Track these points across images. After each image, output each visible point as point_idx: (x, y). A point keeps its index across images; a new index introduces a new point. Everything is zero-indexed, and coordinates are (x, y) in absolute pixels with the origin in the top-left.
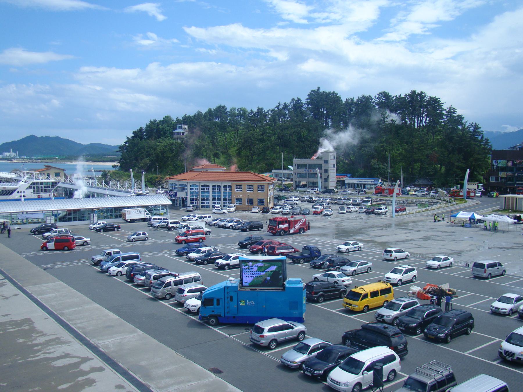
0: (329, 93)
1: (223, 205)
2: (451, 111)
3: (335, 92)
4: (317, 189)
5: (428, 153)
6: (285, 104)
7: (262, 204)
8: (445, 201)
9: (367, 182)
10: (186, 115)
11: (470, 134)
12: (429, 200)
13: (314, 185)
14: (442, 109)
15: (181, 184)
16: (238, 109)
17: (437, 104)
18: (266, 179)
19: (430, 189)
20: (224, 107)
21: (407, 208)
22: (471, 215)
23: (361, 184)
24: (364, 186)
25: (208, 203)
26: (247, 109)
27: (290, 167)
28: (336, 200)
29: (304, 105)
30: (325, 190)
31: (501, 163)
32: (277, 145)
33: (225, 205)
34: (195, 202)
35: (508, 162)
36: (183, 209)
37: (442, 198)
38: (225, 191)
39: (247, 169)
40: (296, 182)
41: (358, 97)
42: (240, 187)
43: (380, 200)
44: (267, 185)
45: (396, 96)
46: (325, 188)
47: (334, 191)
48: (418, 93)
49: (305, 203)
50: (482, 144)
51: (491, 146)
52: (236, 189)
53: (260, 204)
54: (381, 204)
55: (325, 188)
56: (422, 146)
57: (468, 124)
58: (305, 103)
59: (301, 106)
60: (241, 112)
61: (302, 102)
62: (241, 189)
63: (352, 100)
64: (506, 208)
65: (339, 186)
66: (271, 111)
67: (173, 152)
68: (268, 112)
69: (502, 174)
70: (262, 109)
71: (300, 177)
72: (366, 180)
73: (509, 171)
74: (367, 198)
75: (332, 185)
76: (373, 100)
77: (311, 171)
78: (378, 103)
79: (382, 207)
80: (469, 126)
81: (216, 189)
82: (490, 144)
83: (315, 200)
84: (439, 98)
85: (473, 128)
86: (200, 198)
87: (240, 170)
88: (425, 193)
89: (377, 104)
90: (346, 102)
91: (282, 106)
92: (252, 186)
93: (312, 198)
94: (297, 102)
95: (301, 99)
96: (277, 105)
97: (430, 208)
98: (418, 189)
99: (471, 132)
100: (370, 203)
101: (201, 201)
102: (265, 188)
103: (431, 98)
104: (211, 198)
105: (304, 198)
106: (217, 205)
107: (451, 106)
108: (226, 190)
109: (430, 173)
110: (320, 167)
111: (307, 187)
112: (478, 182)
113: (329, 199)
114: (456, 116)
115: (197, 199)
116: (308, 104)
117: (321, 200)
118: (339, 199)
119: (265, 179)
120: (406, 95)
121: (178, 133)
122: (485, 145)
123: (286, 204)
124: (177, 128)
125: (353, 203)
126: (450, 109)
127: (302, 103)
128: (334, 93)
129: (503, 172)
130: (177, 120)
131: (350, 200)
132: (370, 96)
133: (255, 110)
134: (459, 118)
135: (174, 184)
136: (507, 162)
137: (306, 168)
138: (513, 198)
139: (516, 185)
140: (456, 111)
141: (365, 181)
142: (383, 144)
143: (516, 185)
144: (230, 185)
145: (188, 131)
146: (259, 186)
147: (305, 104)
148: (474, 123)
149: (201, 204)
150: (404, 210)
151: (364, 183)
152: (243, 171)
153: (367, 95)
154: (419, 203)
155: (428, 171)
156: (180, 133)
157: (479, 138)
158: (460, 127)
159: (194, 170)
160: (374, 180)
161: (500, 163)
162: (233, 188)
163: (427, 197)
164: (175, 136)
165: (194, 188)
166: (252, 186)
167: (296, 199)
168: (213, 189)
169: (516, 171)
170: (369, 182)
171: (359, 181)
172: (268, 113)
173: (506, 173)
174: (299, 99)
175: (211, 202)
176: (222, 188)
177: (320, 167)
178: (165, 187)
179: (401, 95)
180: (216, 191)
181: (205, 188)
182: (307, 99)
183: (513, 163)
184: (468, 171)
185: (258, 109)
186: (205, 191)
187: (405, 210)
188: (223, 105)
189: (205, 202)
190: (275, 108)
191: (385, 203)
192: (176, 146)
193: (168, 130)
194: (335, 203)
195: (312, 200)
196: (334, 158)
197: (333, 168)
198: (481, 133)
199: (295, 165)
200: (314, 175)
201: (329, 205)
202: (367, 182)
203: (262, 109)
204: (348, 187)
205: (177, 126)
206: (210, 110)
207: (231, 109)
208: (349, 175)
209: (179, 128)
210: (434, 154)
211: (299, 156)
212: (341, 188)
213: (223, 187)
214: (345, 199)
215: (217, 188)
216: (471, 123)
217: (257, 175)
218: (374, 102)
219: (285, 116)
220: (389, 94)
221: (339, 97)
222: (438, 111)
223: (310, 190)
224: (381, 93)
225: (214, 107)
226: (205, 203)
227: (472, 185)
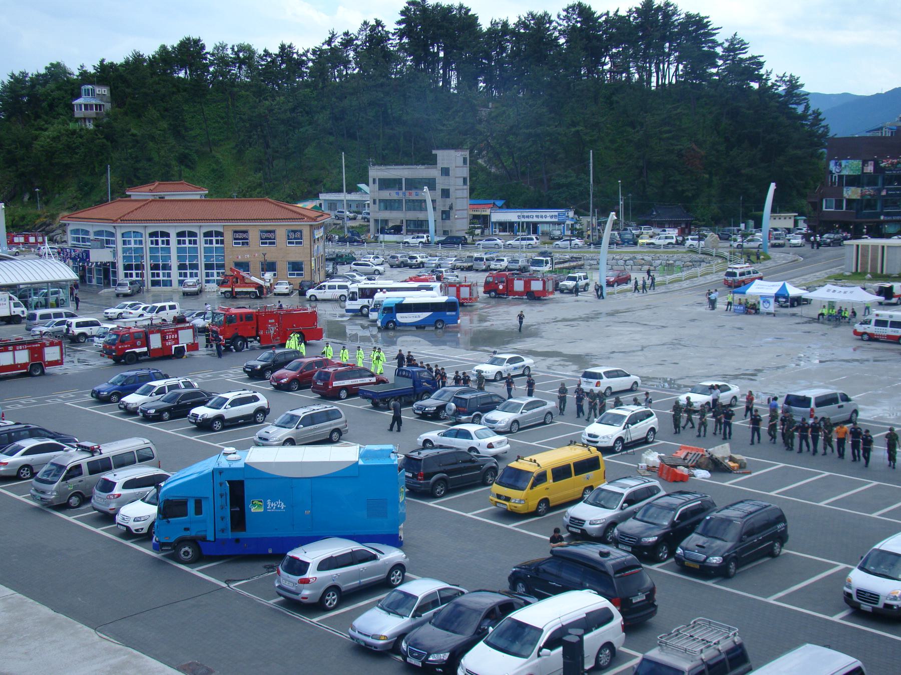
0: (450, 9)
1: (204, 278)
2: (735, 46)
3: (465, 5)
4: (425, 236)
5: (681, 147)
6: (346, 34)
7: (298, 275)
8: (720, 257)
9: (542, 217)
10: (103, 60)
11: (778, 102)
12: (685, 256)
13: (419, 227)
14: (714, 42)
15: (99, 231)
16: (233, 46)
17: (702, 31)
18: (306, 216)
19: (687, 231)
20: (197, 42)
22: (778, 288)
23: (528, 223)
24: (533, 227)
25: (169, 275)
26: (254, 47)
27: (362, 186)
28: (472, 262)
29: (390, 36)
30: (444, 238)
31: (850, 167)
32: (331, 134)
33: (211, 278)
34: (137, 274)
35: (865, 163)
36: (106, 290)
37: (714, 252)
38: (208, 246)
39: (260, 192)
40: (376, 221)
41: (519, 17)
42: (244, 236)
43: (572, 259)
44: (308, 228)
45: (607, 14)
46: (445, 233)
47: (466, 239)
48: (659, 7)
49: (399, 269)
50: (807, 125)
51: (826, 127)
52: (235, 239)
53: (293, 274)
54: (574, 267)
55: (445, 233)
56: (670, 132)
57: (773, 78)
58: (393, 31)
59: (385, 38)
60: (241, 55)
61: (386, 29)
62: (247, 239)
63: (505, 24)
64: (859, 271)
65: (478, 228)
66: (314, 52)
67: (77, 153)
68: (305, 55)
69: (851, 193)
70: (290, 47)
71: (386, 209)
72: (539, 214)
73: (868, 186)
74: (543, 254)
75: (460, 225)
76: (554, 24)
77: (410, 194)
78: (564, 31)
79: (576, 275)
80: (776, 81)
81: (187, 242)
82: (823, 123)
83: (422, 263)
84: (708, 17)
85: (784, 87)
86: (147, 262)
87: (244, 196)
88: (673, 241)
89: (562, 33)
90: (489, 30)
91: (339, 40)
92: (274, 232)
93: (414, 258)
94: (375, 30)
95: (384, 22)
96: (327, 37)
97: (684, 274)
98: (658, 231)
99: (780, 96)
100: (549, 265)
101: (150, 272)
102: (304, 237)
103: (688, 16)
104: (174, 263)
105: (397, 257)
106: (190, 280)
107: (735, 35)
108: (211, 242)
109: (685, 195)
110: (431, 184)
111: (404, 231)
112: (795, 212)
113: (454, 259)
114: (746, 60)
115: (139, 267)
116: (401, 34)
117: (436, 262)
118: (477, 259)
119: (304, 215)
120: (630, 11)
121: (86, 106)
122: (812, 125)
123: (355, 274)
124: (83, 92)
125: (511, 267)
126: (732, 42)
127: (387, 33)
128: (461, 7)
129: (853, 188)
130: (81, 74)
131: (503, 260)
132: (546, 14)
133: (275, 50)
134: (753, 64)
135: (83, 230)
136: (863, 165)
137: (400, 189)
138: (875, 248)
139: (882, 218)
140: (746, 48)
141: (537, 216)
142: (577, 128)
143: (882, 218)
144: (221, 230)
145: (109, 100)
146: (289, 232)
147: (393, 34)
148: (788, 74)
149: (150, 278)
151: (535, 220)
152: (251, 196)
153: (539, 12)
154: (661, 264)
155: (680, 189)
156: (91, 105)
157: (800, 109)
158: (755, 85)
159: (130, 196)
160: (556, 214)
161: (845, 166)
162: (228, 237)
163: (681, 249)
164: (78, 114)
165: (132, 240)
166: (274, 232)
167: (377, 261)
168: (179, 242)
169: (883, 184)
170: (546, 217)
171: (523, 217)
172: (306, 56)
173: (859, 190)
174: (379, 23)
175: (175, 273)
176: (201, 239)
177: (431, 184)
178: (58, 238)
179: (617, 11)
180: (187, 245)
181: (160, 239)
182: (399, 23)
183: (876, 165)
184: (773, 186)
185: (283, 47)
186: (160, 245)
188: (195, 36)
189: (161, 272)
190: (323, 44)
191: (583, 265)
192: (81, 137)
193: (59, 99)
194: (470, 269)
195: (414, 261)
196: (465, 160)
197: (461, 187)
198: (804, 98)
199: (374, 180)
200: (420, 205)
201: (456, 273)
202: (542, 217)
203: (290, 47)
204: (497, 230)
205: (83, 88)
206: (163, 48)
207: (217, 48)
208: (500, 203)
209: (87, 93)
210: (693, 150)
211: (384, 161)
212: (482, 233)
213: (202, 235)
214: (493, 259)
215: (187, 239)
216: (782, 75)
217: (282, 207)
218: (555, 28)
219: (346, 63)
220: (590, 8)
221: (474, 19)
222: (706, 49)
223: (409, 239)
224: (573, 7)
225: (172, 42)
226: (161, 275)
227: (782, 218)
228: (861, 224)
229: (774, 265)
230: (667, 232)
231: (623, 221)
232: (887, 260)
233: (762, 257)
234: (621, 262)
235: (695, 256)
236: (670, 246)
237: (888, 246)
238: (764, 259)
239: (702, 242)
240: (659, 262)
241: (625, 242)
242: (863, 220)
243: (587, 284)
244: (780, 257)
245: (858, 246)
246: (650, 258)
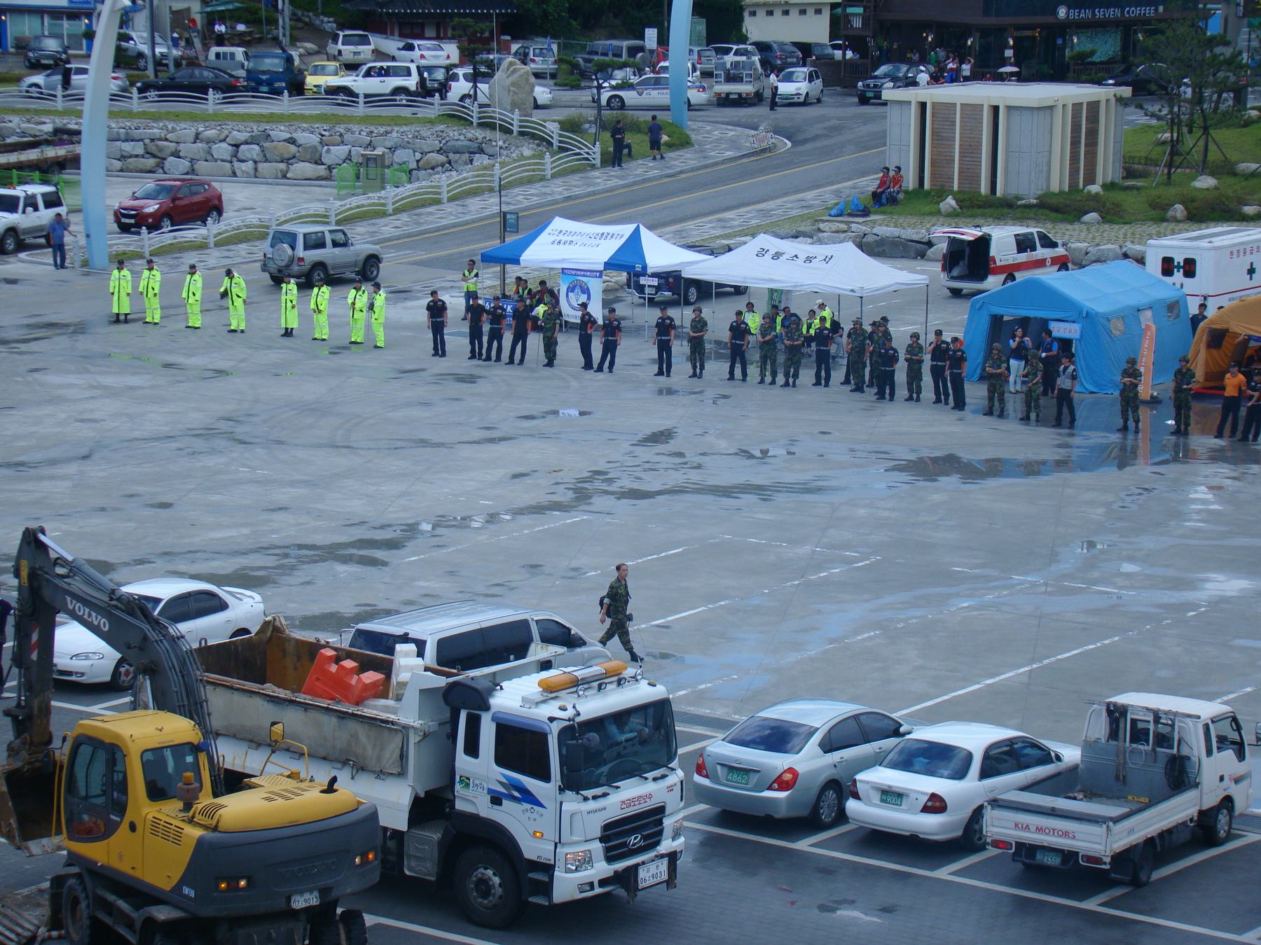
8: (533, 136)
12: (425, 132)
21: (235, 195)
22: (619, 243)
54: (62, 164)
64: (927, 186)
79: (19, 191)
88: (412, 83)
98: (391, 45)
138: (971, 110)
143: (1062, 12)
150: (210, 207)
154: (349, 158)
187: (219, 210)
228: (1001, 31)
229: (693, 163)
230: (417, 53)
231: (288, 10)
232: (1007, 152)
233: (665, 138)
234: (223, 150)
235: (457, 135)
236: (403, 99)
237: (1009, 108)
238: (670, 146)
239: (483, 87)
240: (341, 151)
241: (260, 83)
242: (1009, 20)
243: (60, 223)
244: (719, 140)
245: (923, 106)
246: (314, 139)
